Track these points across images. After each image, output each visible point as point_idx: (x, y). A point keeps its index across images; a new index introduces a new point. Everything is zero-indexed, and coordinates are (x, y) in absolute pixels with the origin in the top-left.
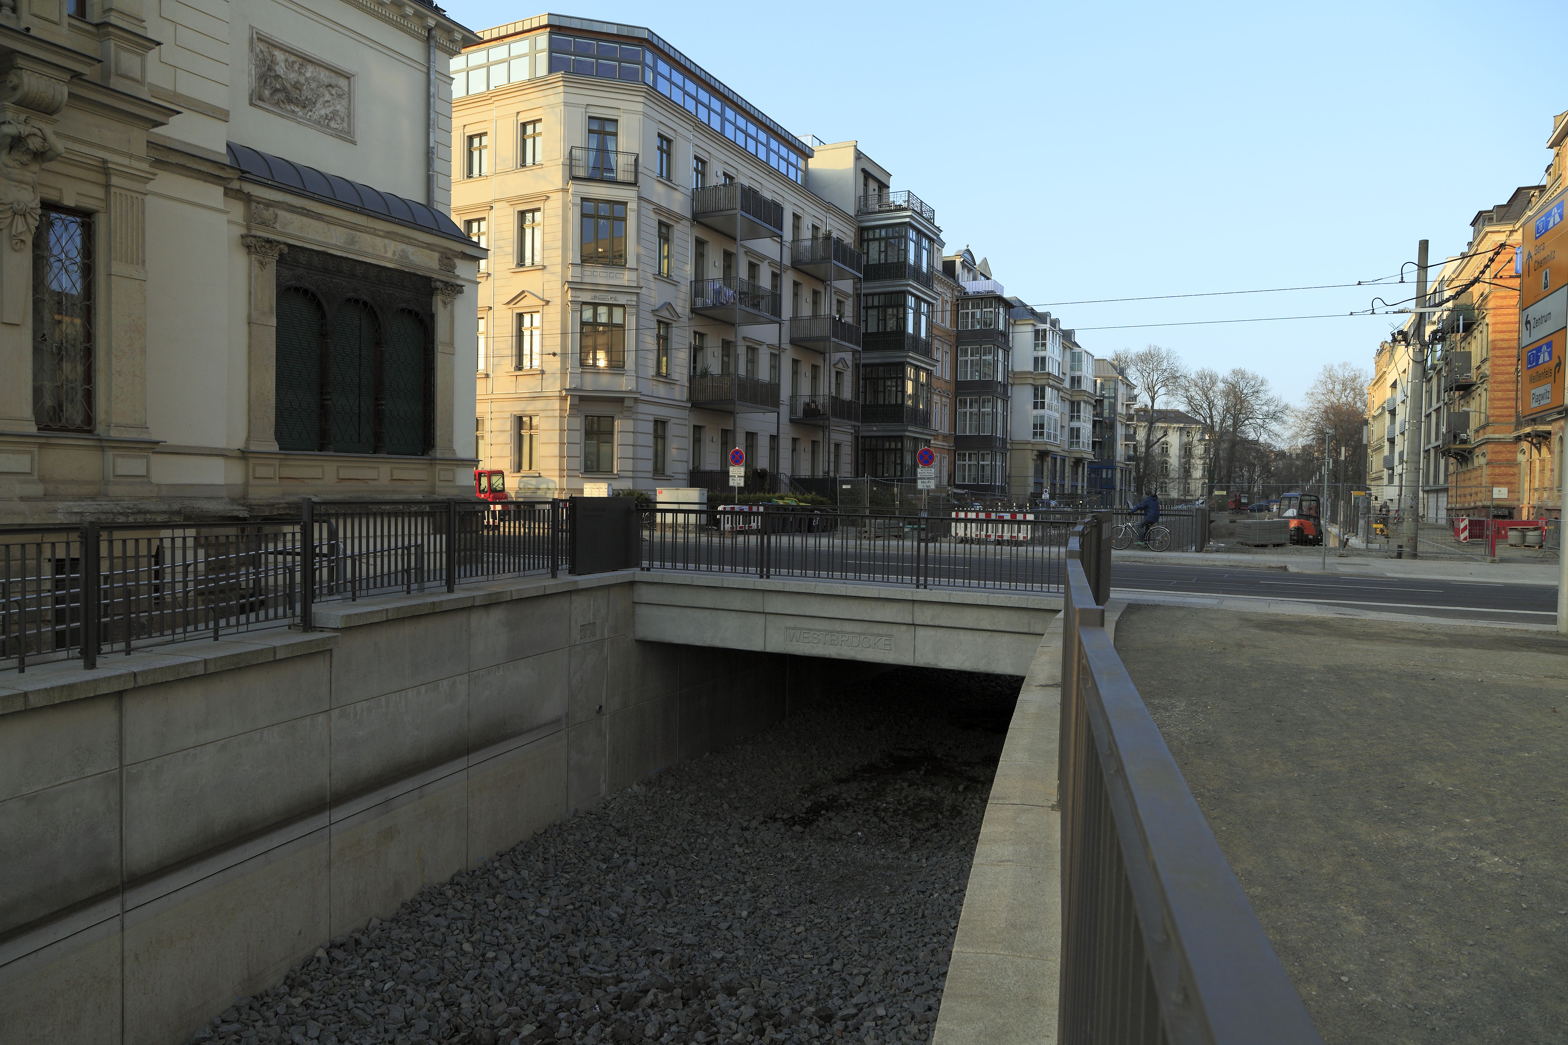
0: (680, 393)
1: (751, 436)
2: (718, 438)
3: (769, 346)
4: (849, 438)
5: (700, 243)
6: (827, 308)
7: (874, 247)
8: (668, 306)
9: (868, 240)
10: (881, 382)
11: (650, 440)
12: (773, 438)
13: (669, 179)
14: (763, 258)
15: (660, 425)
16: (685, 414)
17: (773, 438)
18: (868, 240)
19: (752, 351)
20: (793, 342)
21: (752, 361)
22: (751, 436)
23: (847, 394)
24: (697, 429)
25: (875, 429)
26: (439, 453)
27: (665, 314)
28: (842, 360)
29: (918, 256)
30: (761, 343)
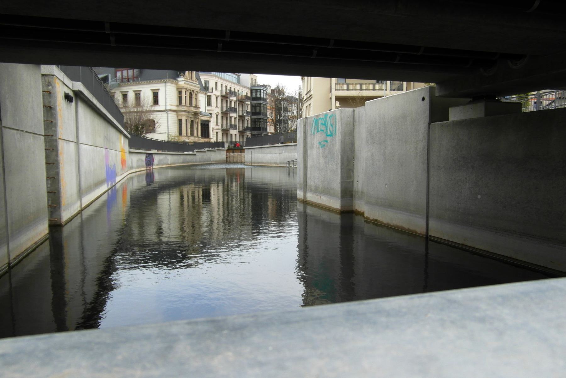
0: (220, 127)
1: (231, 134)
2: (226, 135)
3: (234, 117)
4: (250, 134)
5: (222, 99)
6: (245, 109)
7: (254, 94)
8: (218, 112)
9: (253, 92)
10: (256, 122)
11: (215, 136)
12: (235, 135)
13: (217, 90)
14: (232, 100)
15: (217, 133)
16: (221, 131)
17: (235, 135)
18: (253, 92)
19: (231, 118)
20: (238, 116)
21: (231, 121)
22: (231, 134)
23: (249, 126)
24: (222, 133)
25: (255, 132)
26: (210, 138)
27: (217, 114)
28: (248, 118)
29: (264, 95)
30: (233, 117)
